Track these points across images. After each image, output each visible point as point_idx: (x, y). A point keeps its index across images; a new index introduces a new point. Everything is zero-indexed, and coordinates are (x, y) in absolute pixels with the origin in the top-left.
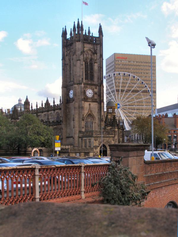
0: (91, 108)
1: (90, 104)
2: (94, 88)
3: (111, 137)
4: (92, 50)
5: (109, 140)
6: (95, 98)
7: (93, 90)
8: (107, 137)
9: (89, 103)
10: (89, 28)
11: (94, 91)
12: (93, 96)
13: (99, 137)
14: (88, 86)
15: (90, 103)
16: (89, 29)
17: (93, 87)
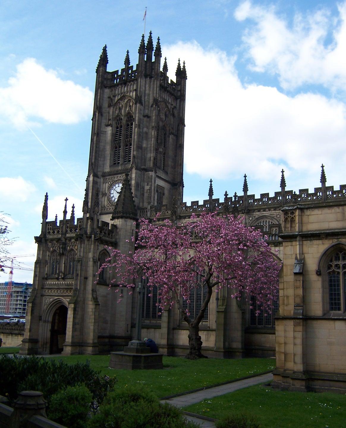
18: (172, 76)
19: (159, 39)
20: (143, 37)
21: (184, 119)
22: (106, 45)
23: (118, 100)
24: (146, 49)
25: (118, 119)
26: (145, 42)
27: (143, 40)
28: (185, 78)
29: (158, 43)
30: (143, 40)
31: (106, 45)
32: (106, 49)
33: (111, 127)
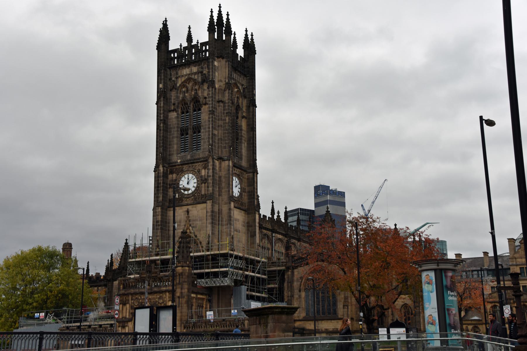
0: (190, 221)
1: (188, 212)
2: (200, 168)
3: (165, 291)
4: (196, 77)
5: (161, 301)
6: (203, 193)
7: (197, 174)
8: (156, 292)
9: (185, 208)
10: (189, 28)
11: (201, 177)
12: (198, 189)
13: (132, 294)
14: (185, 167)
15: (190, 207)
16: (189, 32)
17: (199, 166)
18: (240, 52)
19: (228, 15)
20: (212, 12)
21: (255, 100)
22: (166, 19)
23: (182, 83)
24: (216, 25)
25: (184, 102)
26: (214, 18)
27: (212, 16)
28: (254, 52)
29: (228, 19)
30: (212, 16)
31: (166, 19)
32: (166, 23)
33: (176, 112)
